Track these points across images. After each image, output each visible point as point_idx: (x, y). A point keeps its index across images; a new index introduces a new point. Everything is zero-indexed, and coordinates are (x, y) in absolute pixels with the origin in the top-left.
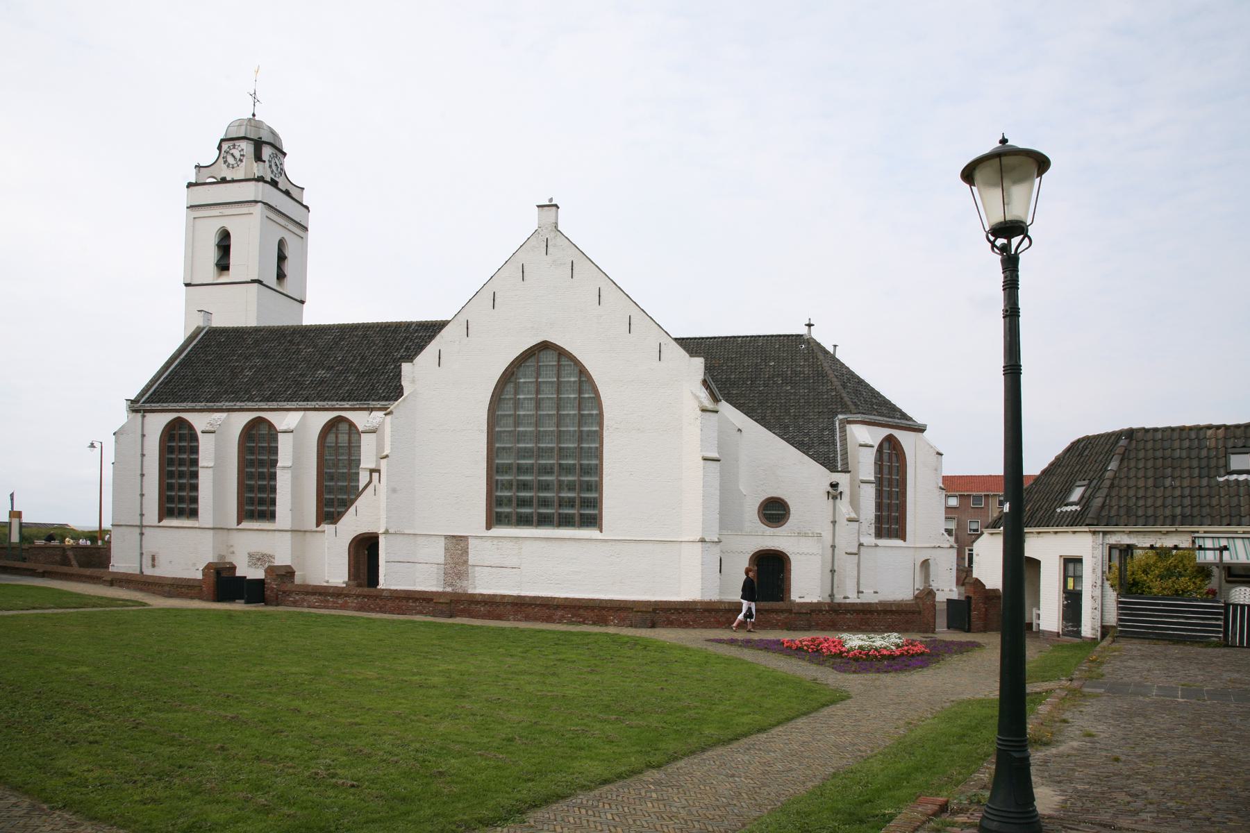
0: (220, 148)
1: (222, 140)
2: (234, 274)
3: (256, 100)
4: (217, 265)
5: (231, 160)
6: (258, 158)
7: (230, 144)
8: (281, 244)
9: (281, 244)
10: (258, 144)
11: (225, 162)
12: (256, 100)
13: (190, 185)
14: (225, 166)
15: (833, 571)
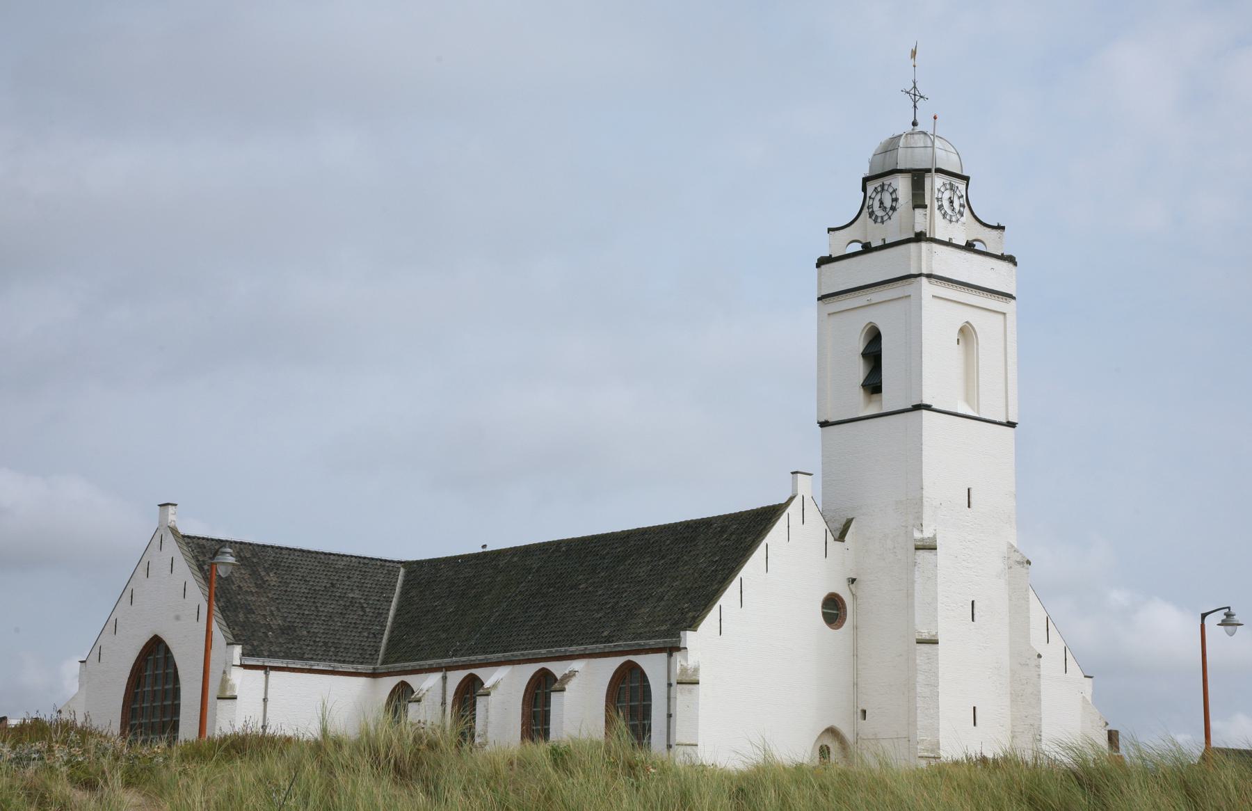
0: (864, 189)
1: (866, 180)
2: (891, 397)
3: (915, 95)
4: (864, 386)
5: (879, 213)
6: (918, 202)
7: (877, 183)
8: (966, 332)
9: (966, 332)
10: (918, 177)
11: (871, 214)
12: (915, 95)
13: (822, 262)
14: (870, 221)
15: (856, 685)
